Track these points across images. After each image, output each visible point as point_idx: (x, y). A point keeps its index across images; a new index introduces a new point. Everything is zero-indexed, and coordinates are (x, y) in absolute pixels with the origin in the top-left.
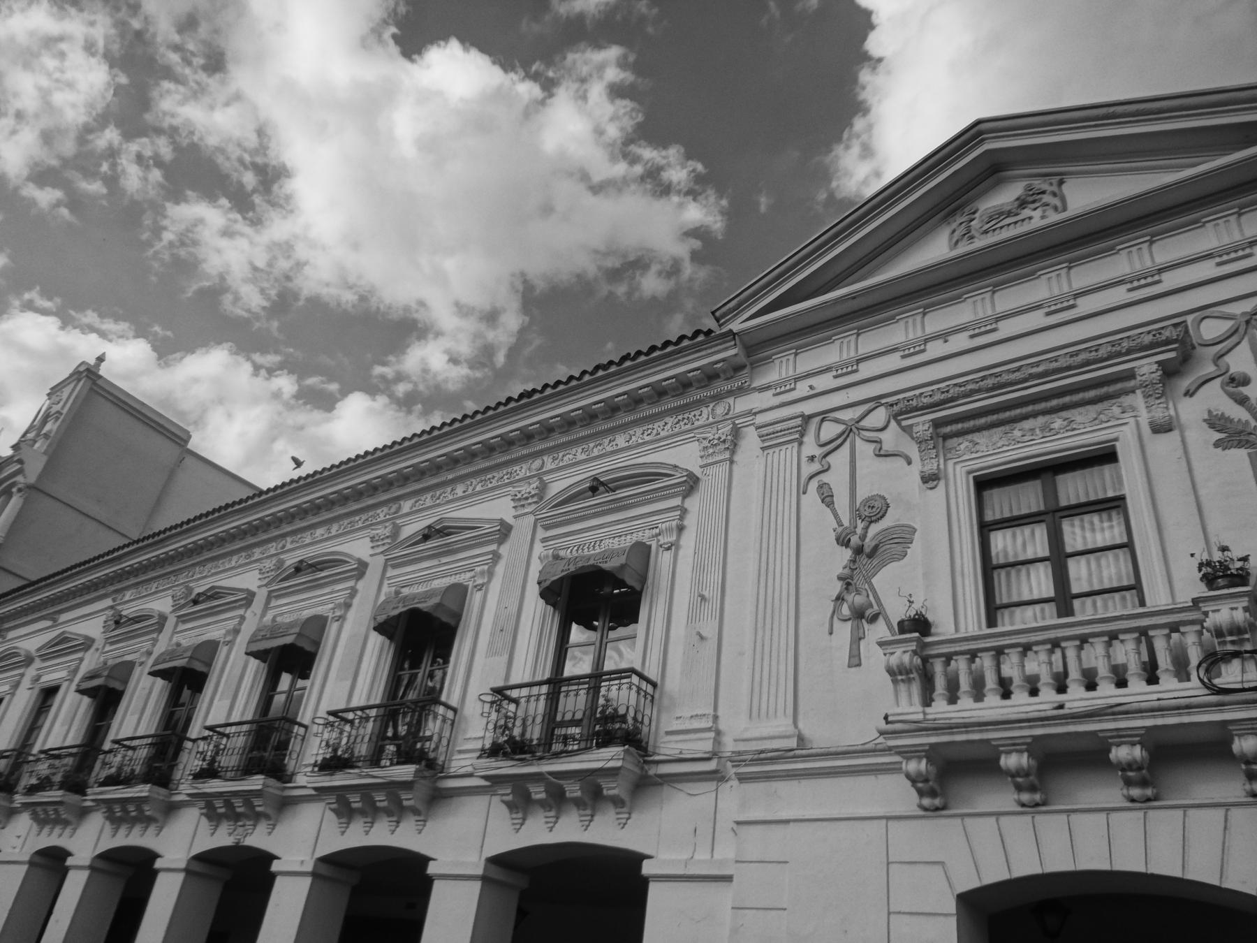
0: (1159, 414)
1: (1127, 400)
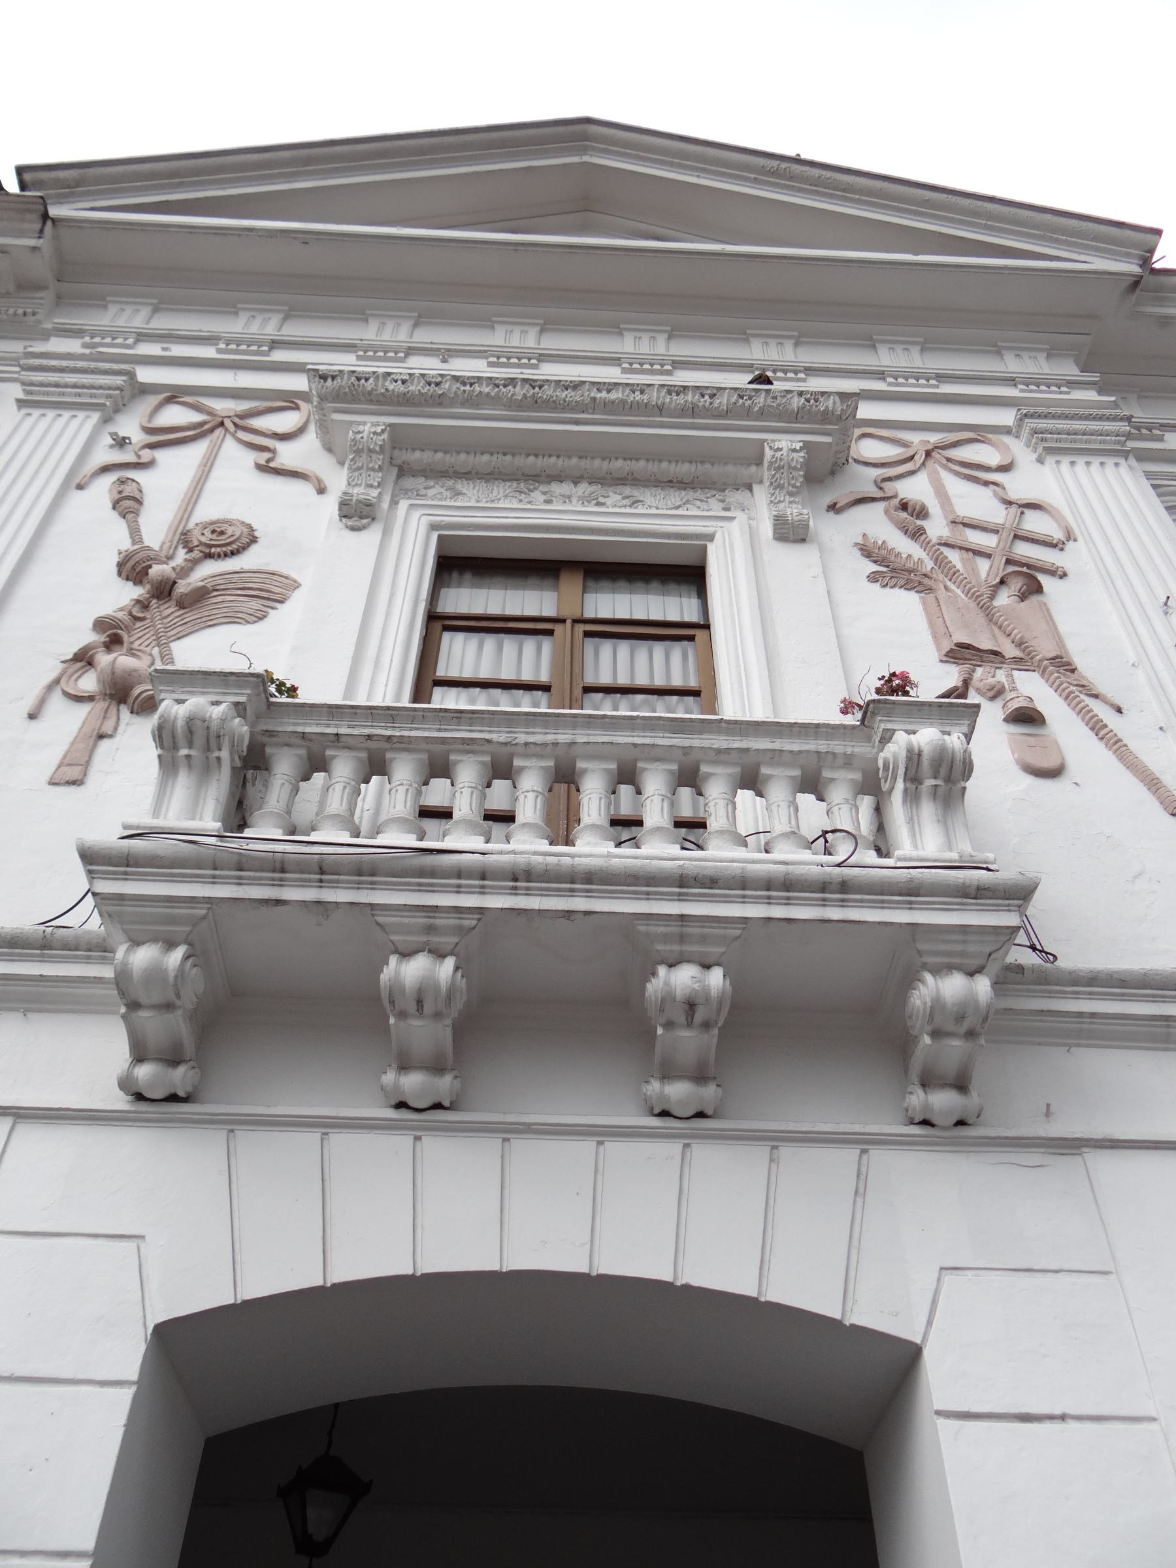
0: (793, 511)
1: (734, 497)
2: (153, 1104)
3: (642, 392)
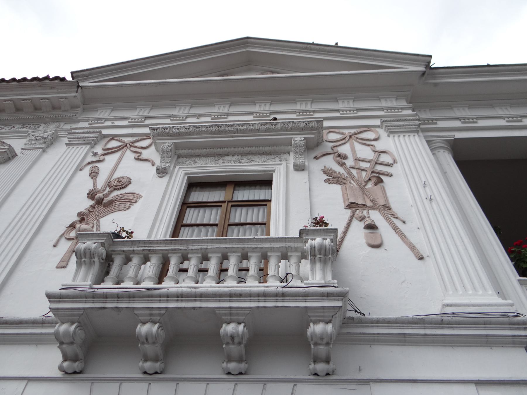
0: (299, 161)
1: (284, 156)
2: (71, 374)
3: (253, 126)
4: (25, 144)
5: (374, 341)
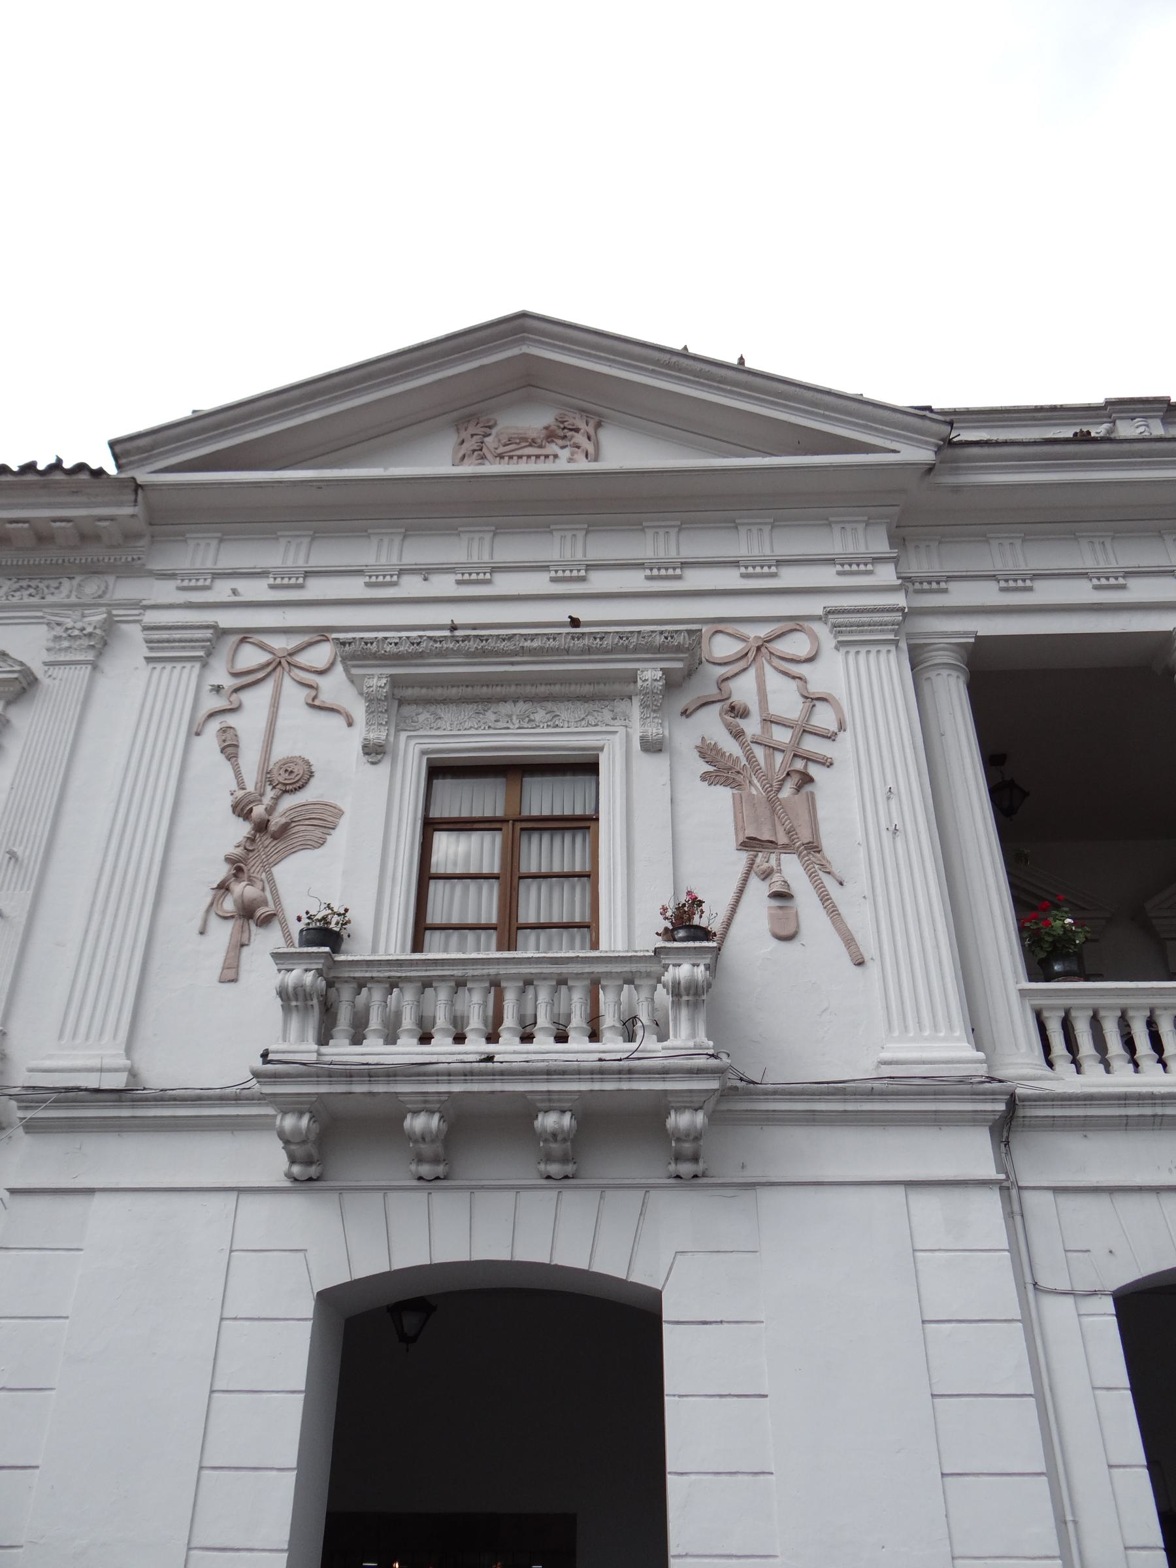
0: (653, 730)
1: (621, 706)
3: (554, 639)
4: (48, 650)
5: (768, 1120)
